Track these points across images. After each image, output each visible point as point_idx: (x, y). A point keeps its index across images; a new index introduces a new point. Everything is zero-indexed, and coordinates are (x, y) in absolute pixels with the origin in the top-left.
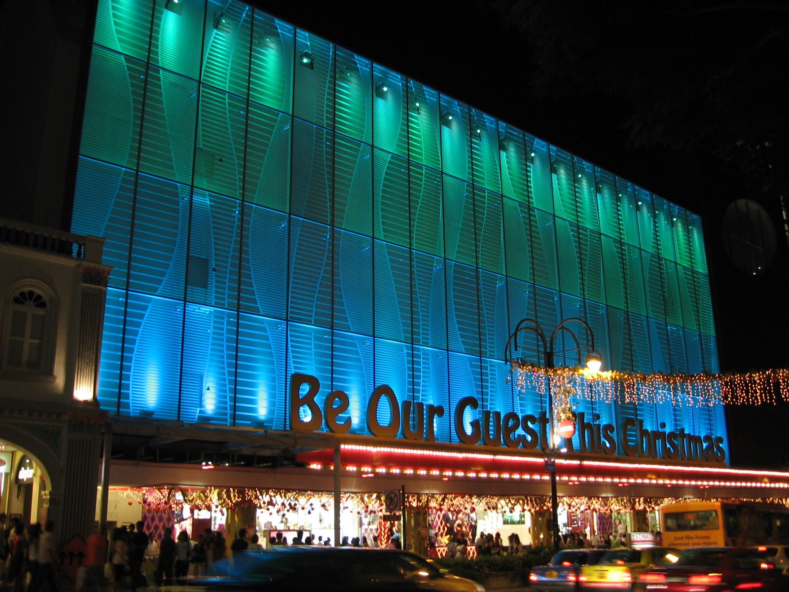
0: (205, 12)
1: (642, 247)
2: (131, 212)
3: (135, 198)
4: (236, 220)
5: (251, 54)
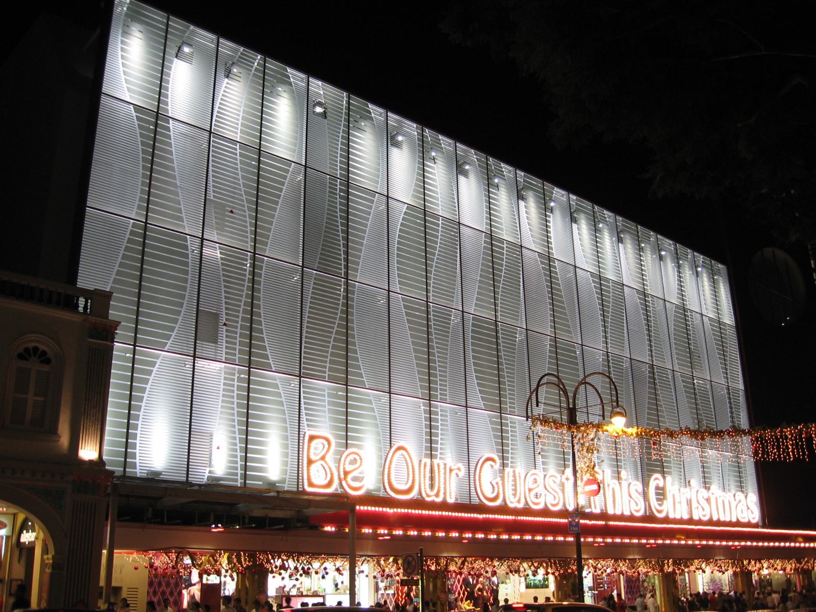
0: (203, 225)
1: (666, 299)
2: (137, 291)
5: (261, 136)
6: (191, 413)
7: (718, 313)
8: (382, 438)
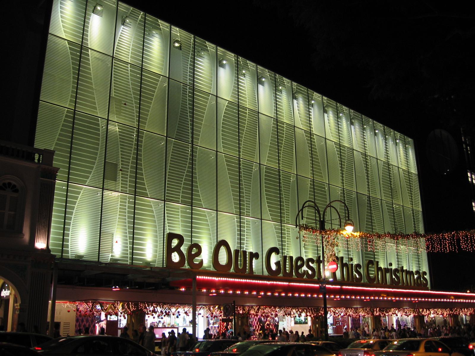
1: (378, 158)
3: (71, 146)
4: (129, 259)
6: (100, 237)
7: (408, 167)
8: (212, 237)
